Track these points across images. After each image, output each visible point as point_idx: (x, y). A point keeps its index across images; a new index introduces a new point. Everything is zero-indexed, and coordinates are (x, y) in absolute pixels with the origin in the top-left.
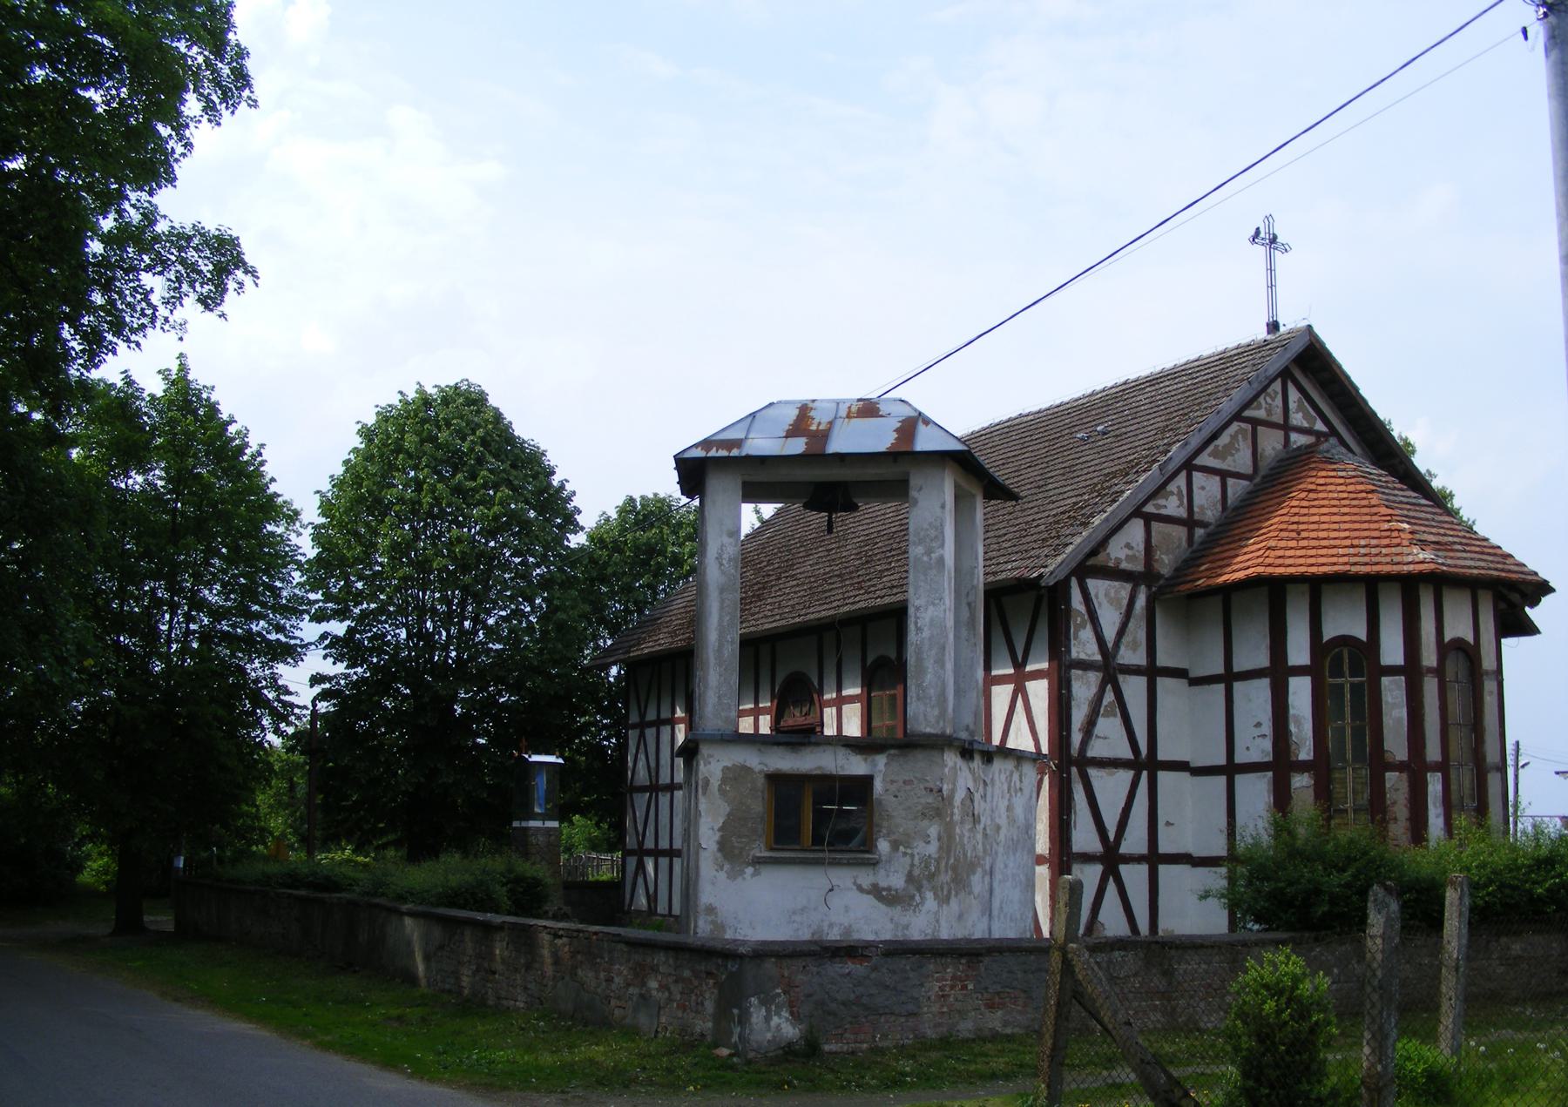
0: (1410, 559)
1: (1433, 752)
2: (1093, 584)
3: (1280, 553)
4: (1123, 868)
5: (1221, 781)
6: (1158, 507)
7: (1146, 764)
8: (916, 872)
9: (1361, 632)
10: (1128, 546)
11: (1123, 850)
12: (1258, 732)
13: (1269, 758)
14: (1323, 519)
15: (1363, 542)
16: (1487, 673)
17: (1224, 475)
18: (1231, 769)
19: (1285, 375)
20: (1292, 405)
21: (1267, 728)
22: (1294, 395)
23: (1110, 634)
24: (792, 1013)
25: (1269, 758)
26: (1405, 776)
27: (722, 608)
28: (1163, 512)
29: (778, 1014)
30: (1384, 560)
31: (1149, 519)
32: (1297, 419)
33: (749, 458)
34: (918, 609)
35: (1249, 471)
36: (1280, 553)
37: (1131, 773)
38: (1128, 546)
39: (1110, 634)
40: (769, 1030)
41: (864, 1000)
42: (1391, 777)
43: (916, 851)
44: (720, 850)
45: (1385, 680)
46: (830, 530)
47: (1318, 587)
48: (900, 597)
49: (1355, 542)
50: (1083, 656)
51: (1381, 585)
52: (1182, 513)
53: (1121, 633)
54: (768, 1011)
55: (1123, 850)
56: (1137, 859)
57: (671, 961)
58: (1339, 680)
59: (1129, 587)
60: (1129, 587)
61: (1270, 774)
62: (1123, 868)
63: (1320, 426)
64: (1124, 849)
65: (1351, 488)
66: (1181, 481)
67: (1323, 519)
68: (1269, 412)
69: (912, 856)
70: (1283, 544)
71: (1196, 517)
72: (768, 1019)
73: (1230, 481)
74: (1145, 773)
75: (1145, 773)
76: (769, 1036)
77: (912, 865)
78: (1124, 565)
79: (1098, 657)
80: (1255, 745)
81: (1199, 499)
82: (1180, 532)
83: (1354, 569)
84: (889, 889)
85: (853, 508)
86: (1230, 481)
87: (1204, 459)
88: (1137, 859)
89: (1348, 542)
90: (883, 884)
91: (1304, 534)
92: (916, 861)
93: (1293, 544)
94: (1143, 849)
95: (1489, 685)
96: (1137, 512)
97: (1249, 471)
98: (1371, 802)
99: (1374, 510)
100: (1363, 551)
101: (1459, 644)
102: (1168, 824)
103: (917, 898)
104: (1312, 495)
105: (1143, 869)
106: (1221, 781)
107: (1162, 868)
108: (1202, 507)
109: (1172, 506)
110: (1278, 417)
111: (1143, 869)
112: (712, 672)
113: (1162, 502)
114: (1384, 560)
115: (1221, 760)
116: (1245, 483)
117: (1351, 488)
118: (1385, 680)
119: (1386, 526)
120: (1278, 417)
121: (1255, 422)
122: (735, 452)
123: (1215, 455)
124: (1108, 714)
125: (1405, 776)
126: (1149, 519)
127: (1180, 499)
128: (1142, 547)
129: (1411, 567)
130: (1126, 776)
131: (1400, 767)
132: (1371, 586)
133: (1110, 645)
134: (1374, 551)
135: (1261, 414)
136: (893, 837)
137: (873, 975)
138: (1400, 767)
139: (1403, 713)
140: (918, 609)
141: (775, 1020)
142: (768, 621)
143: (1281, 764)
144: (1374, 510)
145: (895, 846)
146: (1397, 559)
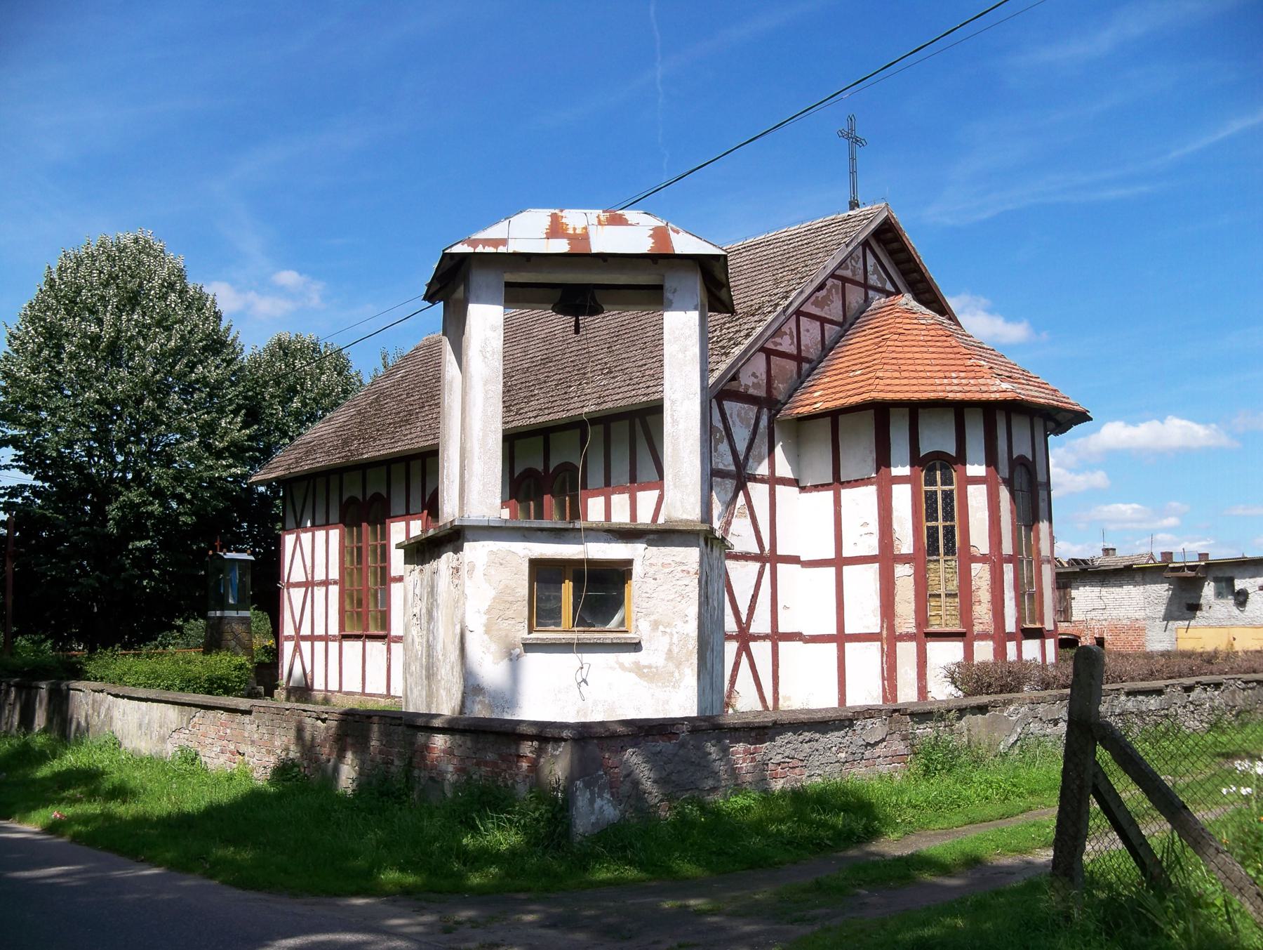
0: (995, 389)
1: (1007, 548)
2: (727, 405)
3: (888, 381)
4: (752, 644)
5: (831, 571)
6: (776, 344)
7: (769, 558)
8: (676, 650)
9: (951, 450)
10: (754, 375)
11: (751, 631)
12: (866, 530)
13: (876, 552)
14: (917, 356)
15: (954, 375)
16: (1041, 484)
17: (823, 321)
18: (839, 562)
19: (865, 244)
20: (870, 269)
21: (874, 527)
22: (871, 260)
23: (741, 447)
24: (612, 795)
25: (876, 552)
26: (987, 567)
27: (486, 399)
28: (779, 348)
29: (601, 796)
30: (974, 388)
31: (769, 353)
32: (873, 280)
33: (515, 255)
34: (673, 402)
35: (841, 319)
36: (888, 381)
37: (758, 565)
38: (754, 375)
39: (741, 447)
40: (592, 813)
41: (674, 777)
42: (976, 568)
43: (674, 630)
44: (487, 632)
45: (971, 488)
46: (577, 331)
47: (916, 410)
48: (657, 396)
49: (947, 374)
50: (721, 466)
51: (966, 410)
52: (793, 350)
53: (749, 448)
54: (592, 794)
55: (751, 631)
56: (763, 637)
57: (469, 744)
58: (933, 488)
59: (755, 409)
60: (755, 409)
61: (877, 565)
62: (752, 644)
63: (889, 287)
64: (753, 630)
65: (932, 333)
66: (792, 323)
67: (917, 356)
68: (854, 272)
69: (672, 634)
70: (889, 374)
71: (803, 354)
72: (592, 801)
73: (827, 326)
74: (768, 565)
75: (768, 565)
76: (593, 819)
77: (671, 644)
78: (751, 391)
79: (733, 468)
80: (862, 541)
81: (805, 340)
82: (791, 366)
83: (951, 396)
84: (650, 667)
85: (596, 310)
86: (827, 326)
87: (810, 308)
88: (763, 637)
89: (942, 375)
90: (644, 662)
91: (903, 368)
92: (675, 640)
93: (897, 374)
94: (766, 629)
95: (1043, 494)
96: (762, 349)
97: (841, 319)
98: (960, 587)
99: (956, 350)
100: (955, 381)
101: (1022, 458)
102: (786, 607)
103: (676, 674)
104: (902, 337)
105: (768, 645)
106: (831, 571)
107: (781, 644)
108: (806, 346)
109: (786, 345)
110: (860, 278)
111: (768, 645)
112: (476, 460)
113: (778, 340)
114: (974, 388)
115: (831, 555)
116: (837, 328)
117: (932, 333)
118: (971, 488)
119: (969, 362)
120: (860, 278)
121: (844, 280)
122: (502, 249)
123: (816, 304)
124: (742, 515)
125: (987, 567)
126: (769, 353)
127: (792, 338)
128: (764, 376)
129: (997, 396)
130: (754, 567)
131: (983, 559)
132: (958, 410)
133: (742, 458)
134: (964, 381)
135: (848, 273)
136: (652, 618)
137: (681, 752)
138: (983, 559)
139: (985, 515)
140: (673, 402)
141: (598, 802)
142: (531, 417)
143: (886, 558)
144: (956, 350)
145: (655, 625)
146: (984, 388)
